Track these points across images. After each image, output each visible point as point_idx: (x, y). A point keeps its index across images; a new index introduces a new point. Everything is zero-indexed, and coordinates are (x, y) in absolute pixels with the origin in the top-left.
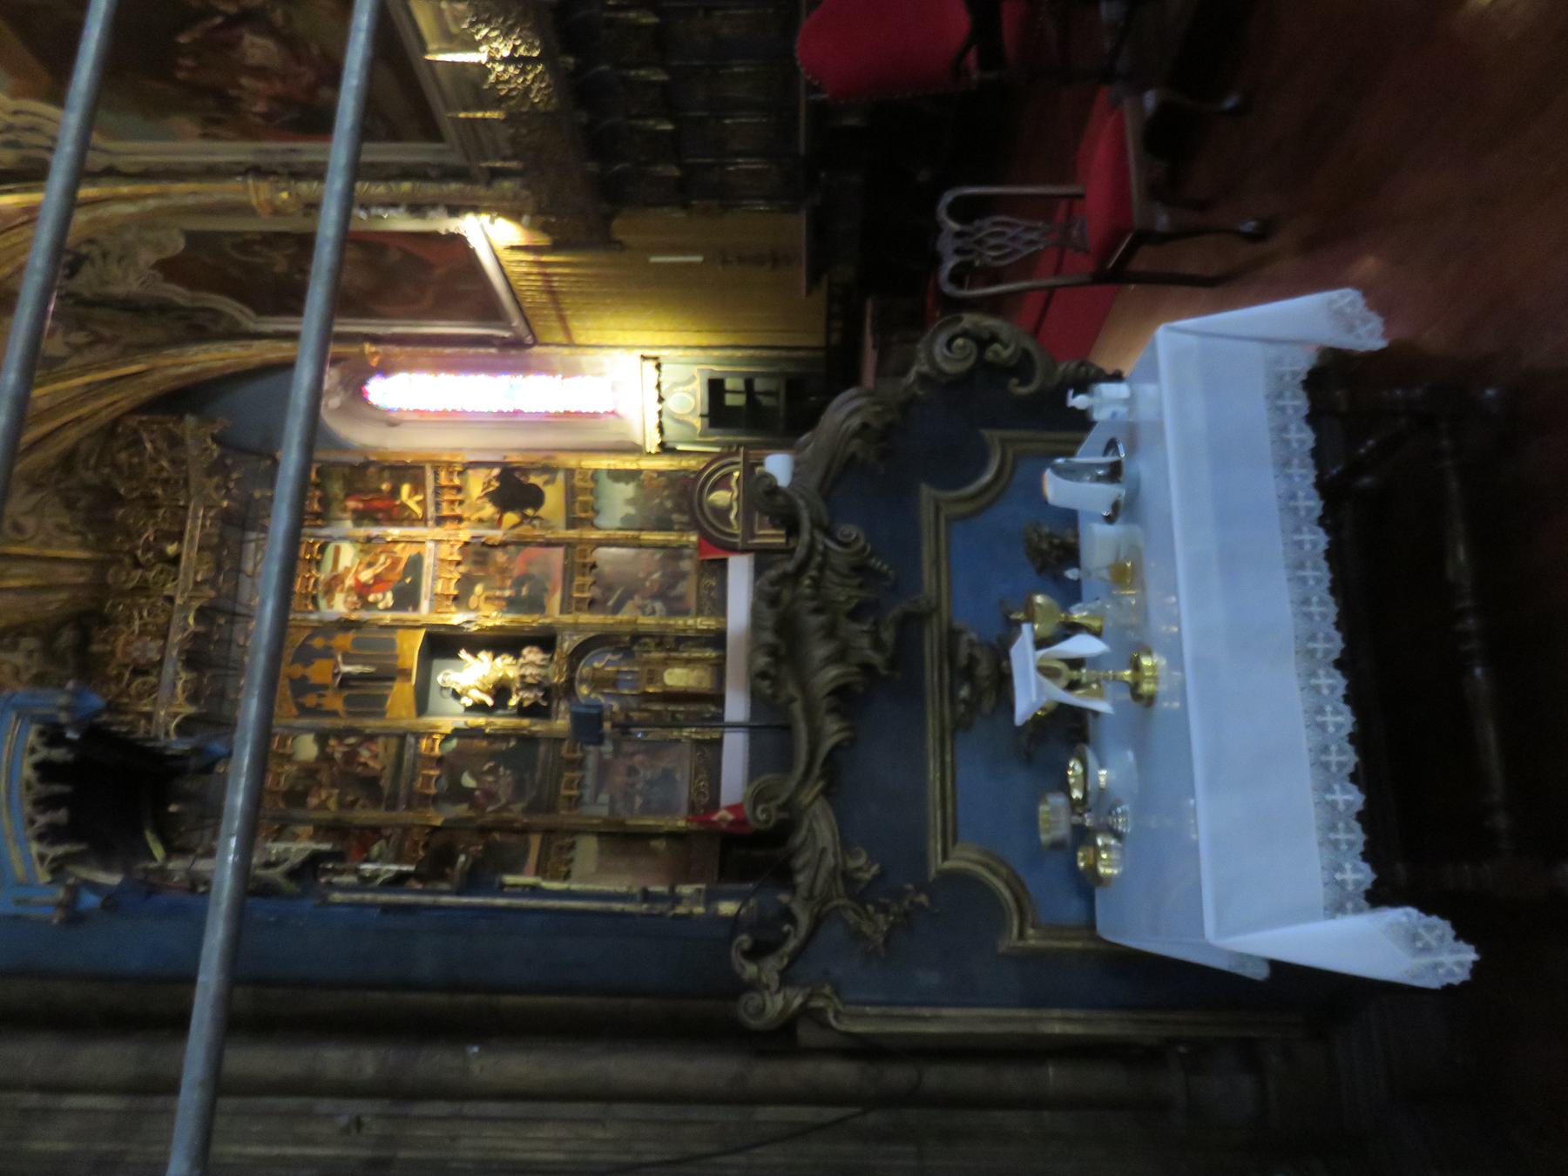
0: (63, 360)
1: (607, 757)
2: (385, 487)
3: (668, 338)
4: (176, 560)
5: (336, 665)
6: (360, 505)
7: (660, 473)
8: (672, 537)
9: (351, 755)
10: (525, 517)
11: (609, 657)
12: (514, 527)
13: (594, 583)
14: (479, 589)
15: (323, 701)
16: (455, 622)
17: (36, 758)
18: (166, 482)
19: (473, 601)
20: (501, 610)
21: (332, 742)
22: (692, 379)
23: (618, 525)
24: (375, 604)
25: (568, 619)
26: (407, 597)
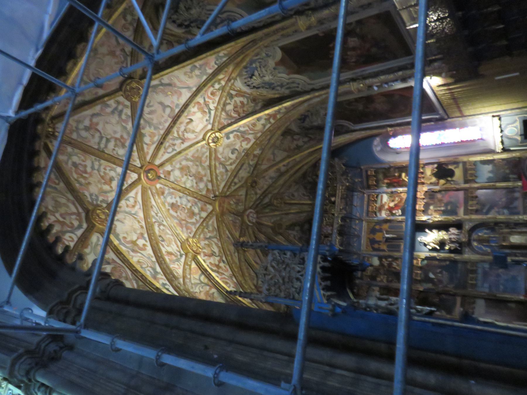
0: (302, 146)
1: (487, 269)
2: (396, 174)
3: (503, 107)
4: (334, 203)
5: (384, 234)
6: (389, 181)
7: (503, 160)
8: (510, 184)
9: (390, 265)
10: (448, 181)
11: (485, 231)
12: (444, 185)
13: (477, 203)
14: (431, 207)
15: (380, 246)
16: (424, 219)
17: (321, 265)
18: (330, 179)
19: (430, 212)
21: (384, 260)
22: (516, 121)
23: (486, 181)
25: (467, 217)
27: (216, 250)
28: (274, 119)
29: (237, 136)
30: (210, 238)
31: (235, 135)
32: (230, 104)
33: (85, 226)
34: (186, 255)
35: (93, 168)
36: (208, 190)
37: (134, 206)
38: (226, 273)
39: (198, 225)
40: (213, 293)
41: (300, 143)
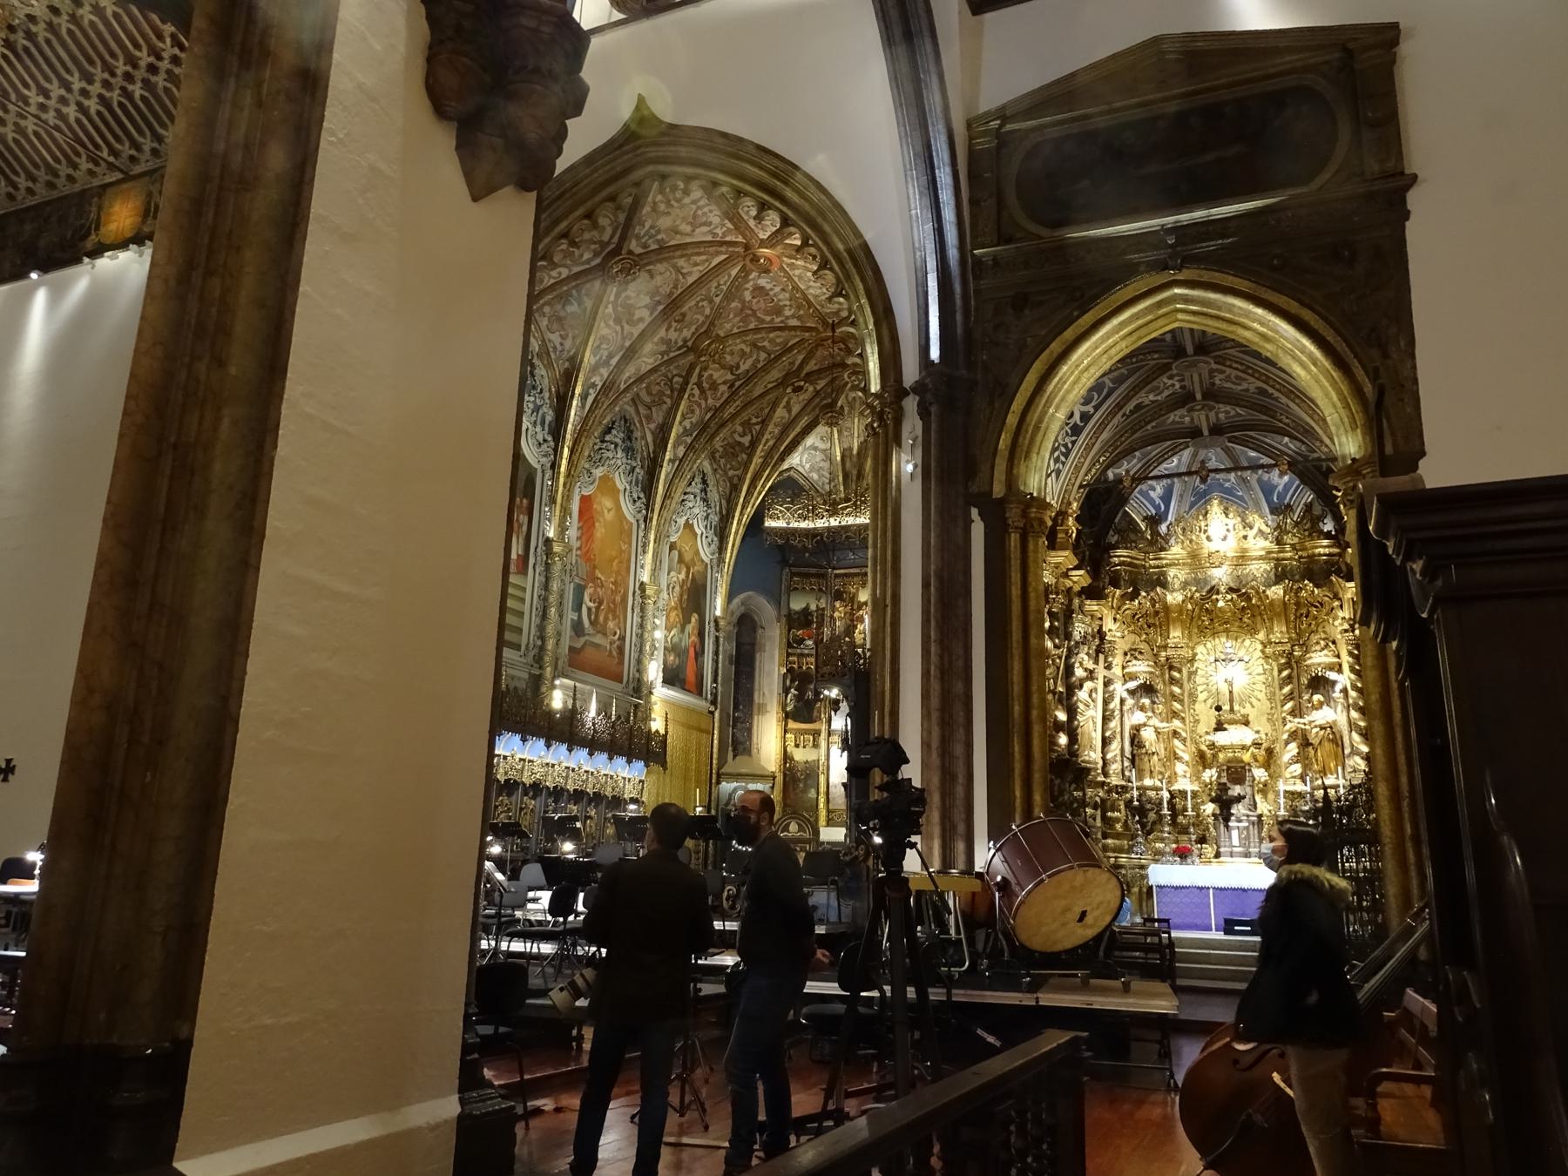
27: (743, 368)
30: (763, 348)
33: (598, 261)
34: (690, 350)
35: (694, 202)
37: (696, 264)
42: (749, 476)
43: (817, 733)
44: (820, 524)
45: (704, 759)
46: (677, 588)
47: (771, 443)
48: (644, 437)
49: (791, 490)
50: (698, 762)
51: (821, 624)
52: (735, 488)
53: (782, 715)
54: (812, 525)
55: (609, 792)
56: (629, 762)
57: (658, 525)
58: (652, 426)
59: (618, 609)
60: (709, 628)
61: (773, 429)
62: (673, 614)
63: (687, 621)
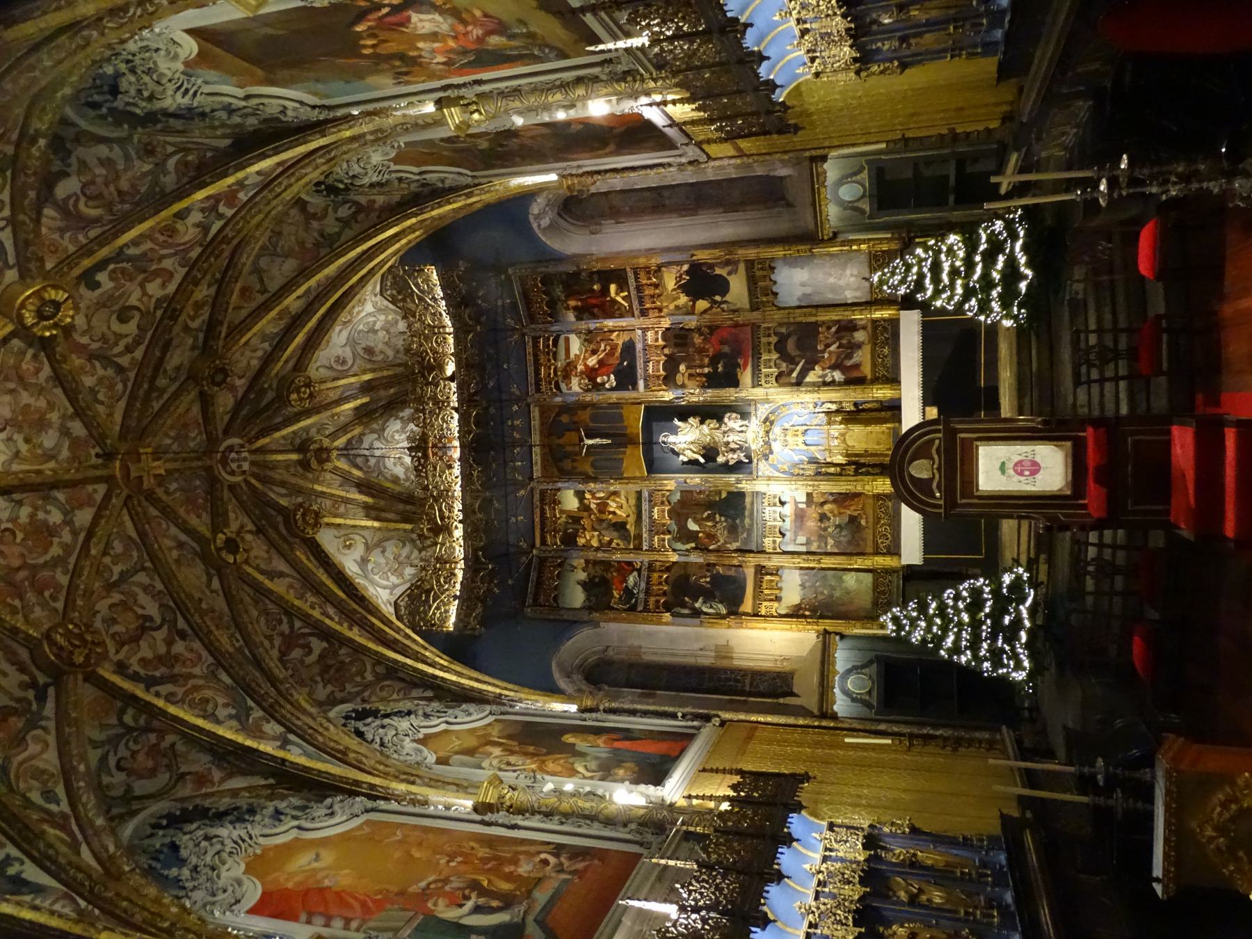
0: (339, 235)
1: (804, 506)
9: (603, 507)
10: (715, 302)
12: (705, 312)
14: (682, 368)
19: (679, 379)
20: (703, 387)
24: (603, 384)
26: (627, 379)
27: (151, 608)
28: (230, 204)
29: (123, 271)
30: (124, 576)
31: (114, 271)
32: (64, 174)
36: (76, 443)
38: (197, 671)
39: (72, 560)
40: (173, 745)
41: (331, 226)
42: (371, 645)
43: (760, 571)
44: (459, 552)
45: (797, 735)
46: (512, 759)
47: (331, 611)
48: (235, 793)
49: (418, 598)
50: (800, 744)
51: (607, 564)
52: (393, 672)
53: (732, 620)
54: (461, 565)
55: (854, 892)
56: (789, 840)
57: (386, 775)
58: (217, 775)
59: (500, 853)
60: (591, 721)
61: (308, 605)
62: (551, 766)
63: (572, 751)
